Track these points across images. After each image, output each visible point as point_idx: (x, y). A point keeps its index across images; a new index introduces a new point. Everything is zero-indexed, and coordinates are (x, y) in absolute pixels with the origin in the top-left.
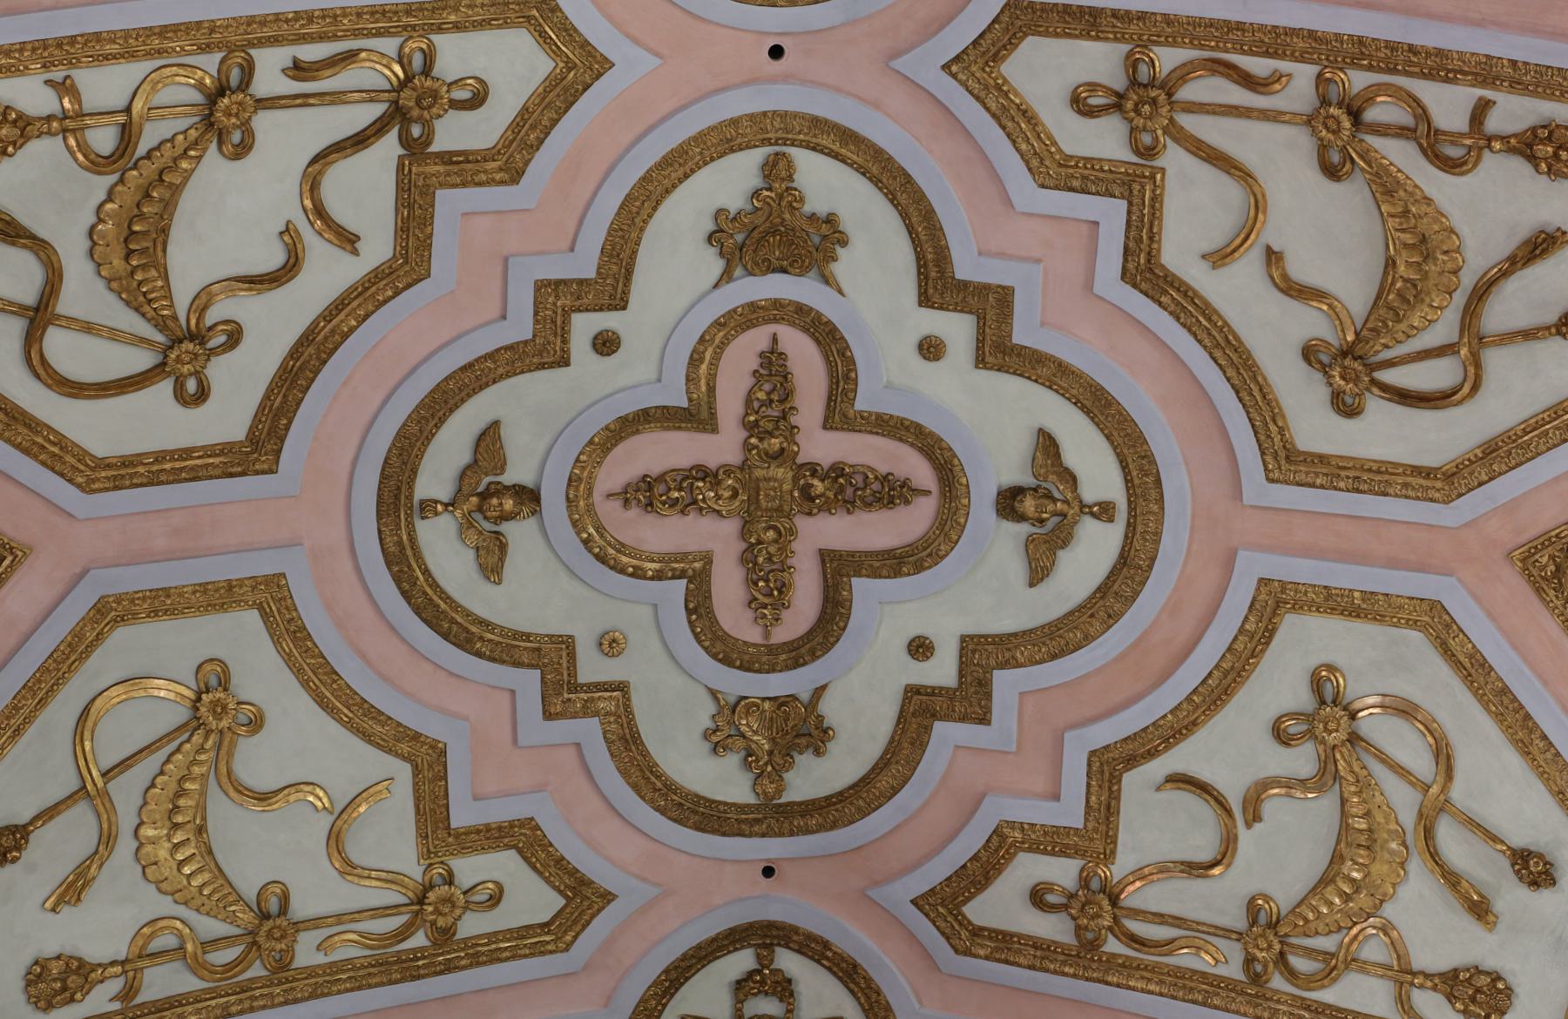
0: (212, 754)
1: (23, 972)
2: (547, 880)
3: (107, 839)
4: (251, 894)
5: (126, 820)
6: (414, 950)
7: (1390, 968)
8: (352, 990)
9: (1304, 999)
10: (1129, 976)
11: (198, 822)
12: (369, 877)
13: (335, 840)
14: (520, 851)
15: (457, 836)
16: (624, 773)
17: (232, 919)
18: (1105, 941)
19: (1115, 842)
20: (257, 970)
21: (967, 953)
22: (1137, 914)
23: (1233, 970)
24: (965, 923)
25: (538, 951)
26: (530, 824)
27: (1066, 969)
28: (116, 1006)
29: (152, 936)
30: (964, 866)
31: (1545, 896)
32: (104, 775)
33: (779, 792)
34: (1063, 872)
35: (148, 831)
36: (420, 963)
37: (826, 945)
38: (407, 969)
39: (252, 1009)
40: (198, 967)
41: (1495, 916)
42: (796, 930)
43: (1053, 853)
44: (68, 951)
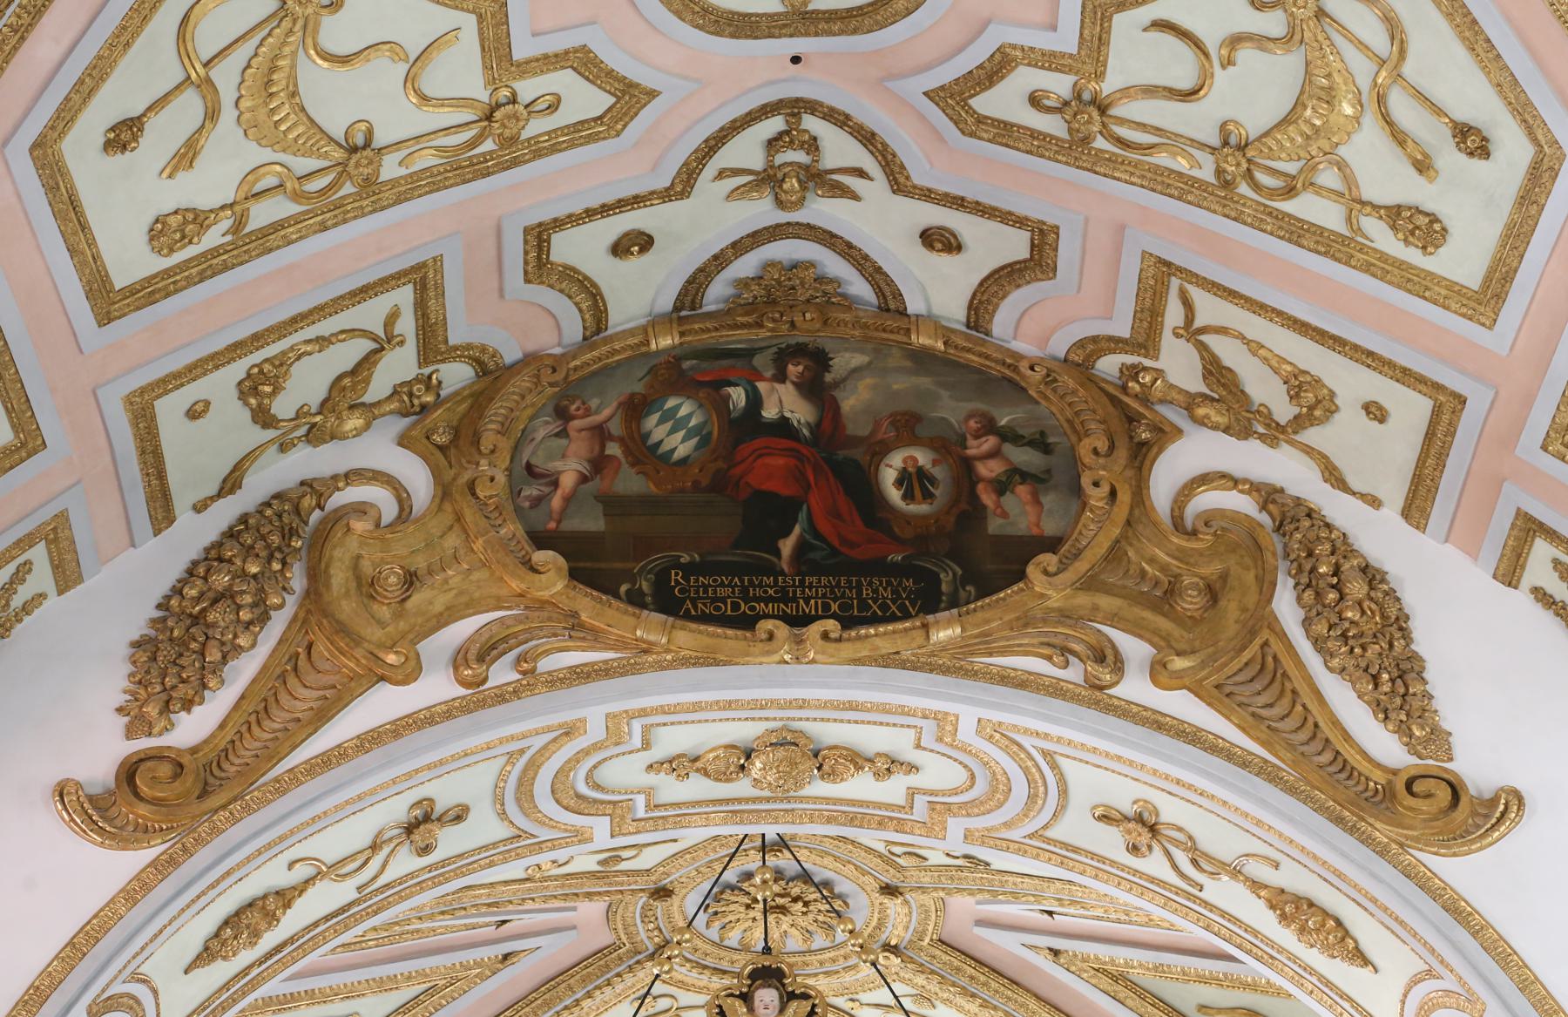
0: (300, 34)
1: (146, 229)
2: (600, 87)
4: (341, 138)
5: (227, 94)
6: (484, 154)
7: (1342, 195)
8: (430, 192)
9: (1266, 206)
10: (1114, 169)
11: (291, 88)
12: (442, 106)
14: (575, 69)
15: (519, 65)
17: (326, 156)
18: (1094, 140)
19: (1105, 66)
20: (348, 189)
21: (972, 135)
22: (1122, 121)
23: (1207, 173)
24: (971, 112)
25: (593, 138)
26: (584, 49)
27: (1060, 158)
28: (229, 238)
29: (257, 180)
30: (971, 72)
31: (1477, 164)
32: (206, 65)
34: (1059, 85)
35: (245, 104)
37: (848, 117)
38: (480, 169)
39: (345, 221)
40: (297, 196)
41: (1437, 172)
42: (821, 104)
43: (1050, 69)
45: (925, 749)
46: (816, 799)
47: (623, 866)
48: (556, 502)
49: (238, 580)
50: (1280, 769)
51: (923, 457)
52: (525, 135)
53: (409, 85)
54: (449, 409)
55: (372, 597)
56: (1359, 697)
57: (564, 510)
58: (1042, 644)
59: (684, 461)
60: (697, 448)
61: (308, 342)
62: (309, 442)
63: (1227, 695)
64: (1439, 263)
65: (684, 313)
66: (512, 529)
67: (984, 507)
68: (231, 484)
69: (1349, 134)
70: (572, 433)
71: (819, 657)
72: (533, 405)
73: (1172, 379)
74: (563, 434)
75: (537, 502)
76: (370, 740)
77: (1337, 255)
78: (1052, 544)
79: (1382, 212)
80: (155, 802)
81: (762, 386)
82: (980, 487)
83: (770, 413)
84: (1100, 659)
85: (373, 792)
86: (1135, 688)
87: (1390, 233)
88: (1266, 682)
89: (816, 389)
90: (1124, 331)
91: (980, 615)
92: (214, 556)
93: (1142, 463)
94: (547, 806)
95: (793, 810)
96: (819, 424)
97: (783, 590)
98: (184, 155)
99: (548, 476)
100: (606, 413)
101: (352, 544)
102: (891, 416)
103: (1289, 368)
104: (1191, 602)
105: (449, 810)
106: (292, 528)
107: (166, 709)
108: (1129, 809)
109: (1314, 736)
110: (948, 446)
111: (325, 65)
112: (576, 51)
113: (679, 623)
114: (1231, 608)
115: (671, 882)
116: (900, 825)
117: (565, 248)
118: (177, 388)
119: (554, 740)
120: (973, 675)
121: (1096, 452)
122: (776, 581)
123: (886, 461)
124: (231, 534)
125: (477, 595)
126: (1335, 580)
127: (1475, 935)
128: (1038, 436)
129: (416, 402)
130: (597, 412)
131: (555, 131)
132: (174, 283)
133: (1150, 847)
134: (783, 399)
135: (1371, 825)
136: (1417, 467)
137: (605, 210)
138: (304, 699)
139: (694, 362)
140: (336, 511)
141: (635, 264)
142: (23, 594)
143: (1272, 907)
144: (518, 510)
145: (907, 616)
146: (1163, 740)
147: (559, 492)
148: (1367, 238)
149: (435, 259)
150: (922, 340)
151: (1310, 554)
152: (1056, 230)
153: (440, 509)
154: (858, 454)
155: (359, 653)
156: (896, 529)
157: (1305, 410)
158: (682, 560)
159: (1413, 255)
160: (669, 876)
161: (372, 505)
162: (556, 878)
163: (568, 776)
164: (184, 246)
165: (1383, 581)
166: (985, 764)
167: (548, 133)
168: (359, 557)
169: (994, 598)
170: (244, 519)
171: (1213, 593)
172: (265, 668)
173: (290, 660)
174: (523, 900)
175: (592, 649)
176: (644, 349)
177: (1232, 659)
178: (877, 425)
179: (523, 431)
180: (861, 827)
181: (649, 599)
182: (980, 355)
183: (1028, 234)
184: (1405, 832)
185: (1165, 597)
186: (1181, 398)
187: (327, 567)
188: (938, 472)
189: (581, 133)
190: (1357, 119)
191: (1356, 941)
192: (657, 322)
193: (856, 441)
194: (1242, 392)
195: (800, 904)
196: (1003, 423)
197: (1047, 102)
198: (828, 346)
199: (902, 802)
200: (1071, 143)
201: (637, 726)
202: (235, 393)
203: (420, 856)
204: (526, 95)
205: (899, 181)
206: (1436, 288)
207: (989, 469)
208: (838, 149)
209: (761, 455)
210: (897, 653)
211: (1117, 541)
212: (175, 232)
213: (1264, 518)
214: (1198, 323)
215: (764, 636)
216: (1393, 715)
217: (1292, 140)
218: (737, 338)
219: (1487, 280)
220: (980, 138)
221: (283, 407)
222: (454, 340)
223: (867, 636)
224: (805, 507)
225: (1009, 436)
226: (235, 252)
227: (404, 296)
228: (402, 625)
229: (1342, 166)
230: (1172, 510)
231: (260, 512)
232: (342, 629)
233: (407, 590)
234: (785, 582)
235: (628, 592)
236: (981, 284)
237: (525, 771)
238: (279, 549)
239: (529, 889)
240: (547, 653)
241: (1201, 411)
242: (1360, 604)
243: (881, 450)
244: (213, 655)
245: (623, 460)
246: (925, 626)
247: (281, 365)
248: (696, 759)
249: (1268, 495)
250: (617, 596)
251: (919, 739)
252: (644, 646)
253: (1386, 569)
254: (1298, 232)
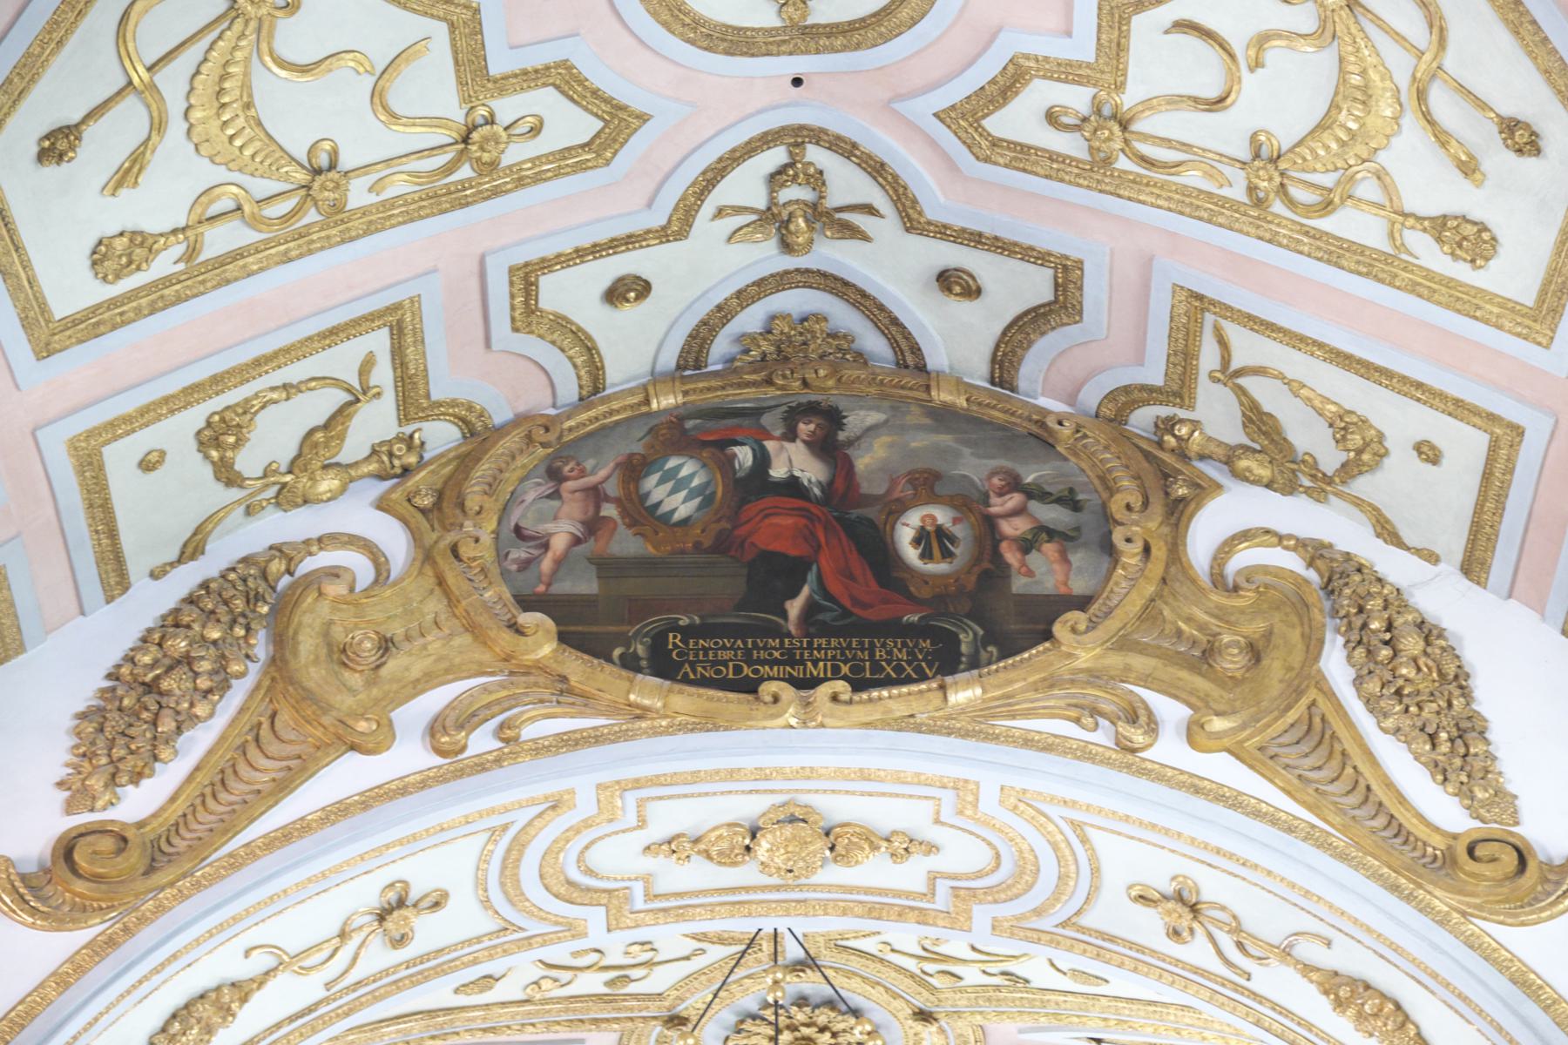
0: (254, 36)
1: (88, 252)
2: (586, 109)
3: (158, 125)
4: (302, 156)
5: (175, 104)
6: (462, 182)
7: (1382, 207)
8: (404, 223)
9: (1302, 225)
10: (1139, 191)
11: (245, 99)
12: (414, 125)
13: (378, 97)
14: (557, 87)
15: (495, 81)
16: (655, 14)
17: (286, 178)
18: (1117, 159)
19: (1125, 75)
20: (312, 216)
21: (987, 160)
22: (1145, 137)
23: (1238, 193)
24: (986, 134)
25: (581, 167)
26: (566, 65)
27: (1081, 181)
28: (181, 266)
29: (211, 202)
30: (982, 88)
31: (1530, 162)
32: (149, 69)
33: (804, 17)
34: (1077, 99)
35: (196, 115)
36: (468, 192)
37: (855, 145)
38: (457, 199)
39: (310, 252)
40: (255, 222)
41: (1484, 175)
43: (1066, 81)
44: (130, 227)
45: (943, 824)
46: (830, 888)
47: (632, 988)
48: (547, 564)
49: (195, 646)
50: (1328, 834)
51: (942, 516)
52: (506, 160)
53: (376, 100)
54: (432, 472)
55: (345, 665)
56: (1416, 759)
57: (555, 572)
58: (1069, 705)
59: (685, 522)
60: (699, 508)
61: (273, 389)
62: (278, 504)
63: (1272, 758)
64: (1492, 278)
65: (688, 373)
66: (496, 593)
67: (1008, 566)
68: (192, 549)
69: (1388, 137)
70: (565, 495)
71: (827, 721)
72: (524, 466)
73: (1210, 432)
74: (556, 495)
75: (525, 565)
76: (338, 812)
77: (1381, 275)
78: (1083, 603)
79: (1426, 223)
80: (97, 878)
81: (770, 445)
82: (1004, 545)
83: (778, 472)
84: (1133, 719)
85: (337, 869)
86: (1170, 749)
87: (1435, 246)
88: (1313, 744)
89: (828, 447)
90: (1157, 379)
91: (1002, 675)
92: (173, 621)
93: (1179, 519)
94: (535, 891)
95: (805, 901)
96: (831, 483)
97: (790, 652)
98: (129, 169)
99: (538, 538)
100: (602, 473)
101: (324, 609)
102: (909, 473)
103: (1333, 408)
104: (1233, 662)
105: (426, 896)
106: (258, 593)
107: (113, 781)
108: (1169, 888)
109: (1366, 800)
110: (969, 503)
111: (283, 73)
112: (557, 65)
113: (677, 687)
114: (1275, 668)
115: (686, 1009)
116: (923, 917)
117: (556, 292)
118: (128, 433)
119: (540, 815)
120: (995, 738)
121: (1128, 507)
122: (782, 643)
123: (903, 519)
124: (191, 600)
125: (457, 660)
126: (1388, 636)
127: (1546, 1009)
128: (1066, 493)
129: (397, 462)
130: (593, 472)
131: (538, 158)
132: (121, 314)
133: (1192, 931)
134: (793, 458)
135: (1429, 893)
136: (1475, 513)
137: (597, 251)
138: (265, 771)
139: (698, 421)
140: (306, 575)
141: (630, 313)
143: (1326, 993)
144: (505, 574)
145: (923, 678)
146: (1200, 805)
147: (550, 555)
148: (1411, 254)
149: (412, 300)
150: (942, 396)
151: (1361, 610)
152: (1079, 264)
153: (420, 573)
154: (871, 512)
155: (326, 720)
156: (912, 589)
157: (1352, 454)
158: (681, 623)
159: (1461, 271)
160: (683, 1000)
161: (346, 569)
162: (559, 1000)
163: (557, 858)
164: (131, 273)
165: (1440, 636)
166: (1012, 840)
167: (532, 160)
168: (331, 623)
169: (1018, 658)
170: (205, 585)
171: (1255, 652)
172: (222, 738)
173: (251, 730)
174: (523, 1025)
175: (581, 715)
176: (644, 409)
177: (1276, 719)
178: (894, 482)
179: (512, 493)
180: (879, 919)
181: (644, 663)
182: (1006, 412)
183: (1051, 272)
184: (1467, 899)
185: (1206, 656)
186: (1220, 452)
187: (296, 633)
188: (959, 531)
189: (567, 161)
190: (1396, 119)
191: (1417, 1027)
192: (658, 380)
193: (871, 500)
194: (1285, 440)
195: (827, 1035)
196: (1029, 479)
197: (1065, 120)
198: (842, 404)
199: (922, 888)
200: (1092, 163)
201: (631, 798)
202: (193, 445)
203: (394, 947)
204: (504, 117)
205: (912, 220)
206: (1488, 306)
207: (1013, 528)
209: (767, 516)
210: (912, 716)
211: (1153, 600)
212: (120, 257)
213: (1312, 575)
214: (1236, 364)
215: (768, 698)
216: (1452, 777)
217: (1327, 148)
218: (746, 397)
219: (1541, 299)
220: (995, 163)
221: (248, 462)
222: (436, 395)
223: (880, 699)
224: (814, 568)
225: (1035, 493)
226: (189, 283)
227: (379, 341)
228: (375, 692)
229: (1380, 175)
230: (1212, 567)
231: (223, 576)
232: (308, 696)
233: (382, 656)
234: (792, 644)
235: (622, 656)
236: (1004, 333)
237: (508, 851)
238: (244, 615)
239: (529, 1013)
240: (532, 719)
241: (1243, 464)
242: (1415, 660)
243: (897, 509)
244: (167, 725)
245: (619, 521)
246: (942, 688)
247: (245, 413)
248: (696, 841)
249: (1315, 552)
250: (609, 660)
251: (938, 813)
252: (638, 712)
253: (1444, 625)
254: (1337, 252)
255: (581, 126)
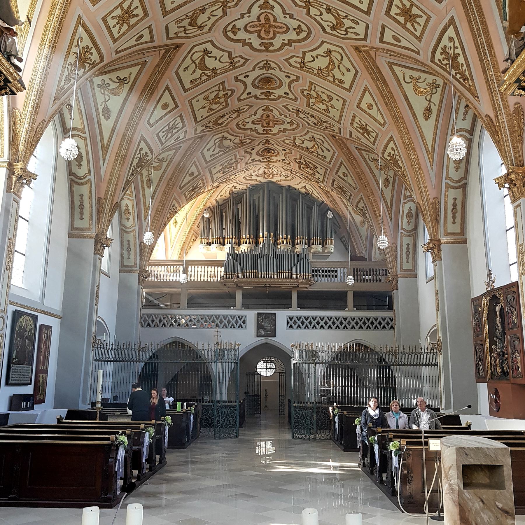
117: (239, 78)
142: (176, 123)
204: (235, 61)
208: (273, 65)
255: (242, 61)
